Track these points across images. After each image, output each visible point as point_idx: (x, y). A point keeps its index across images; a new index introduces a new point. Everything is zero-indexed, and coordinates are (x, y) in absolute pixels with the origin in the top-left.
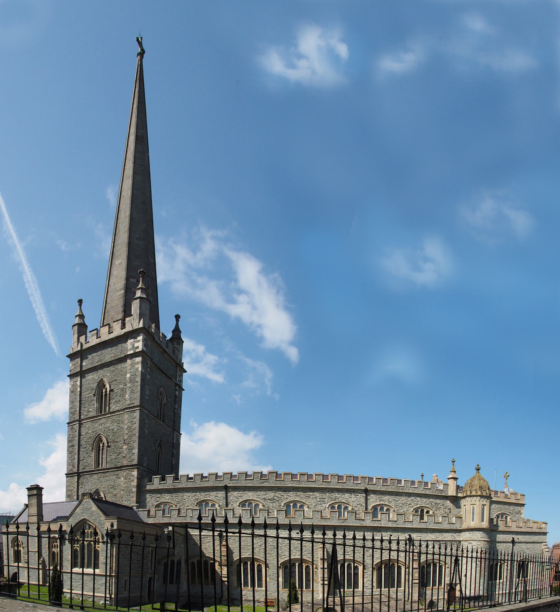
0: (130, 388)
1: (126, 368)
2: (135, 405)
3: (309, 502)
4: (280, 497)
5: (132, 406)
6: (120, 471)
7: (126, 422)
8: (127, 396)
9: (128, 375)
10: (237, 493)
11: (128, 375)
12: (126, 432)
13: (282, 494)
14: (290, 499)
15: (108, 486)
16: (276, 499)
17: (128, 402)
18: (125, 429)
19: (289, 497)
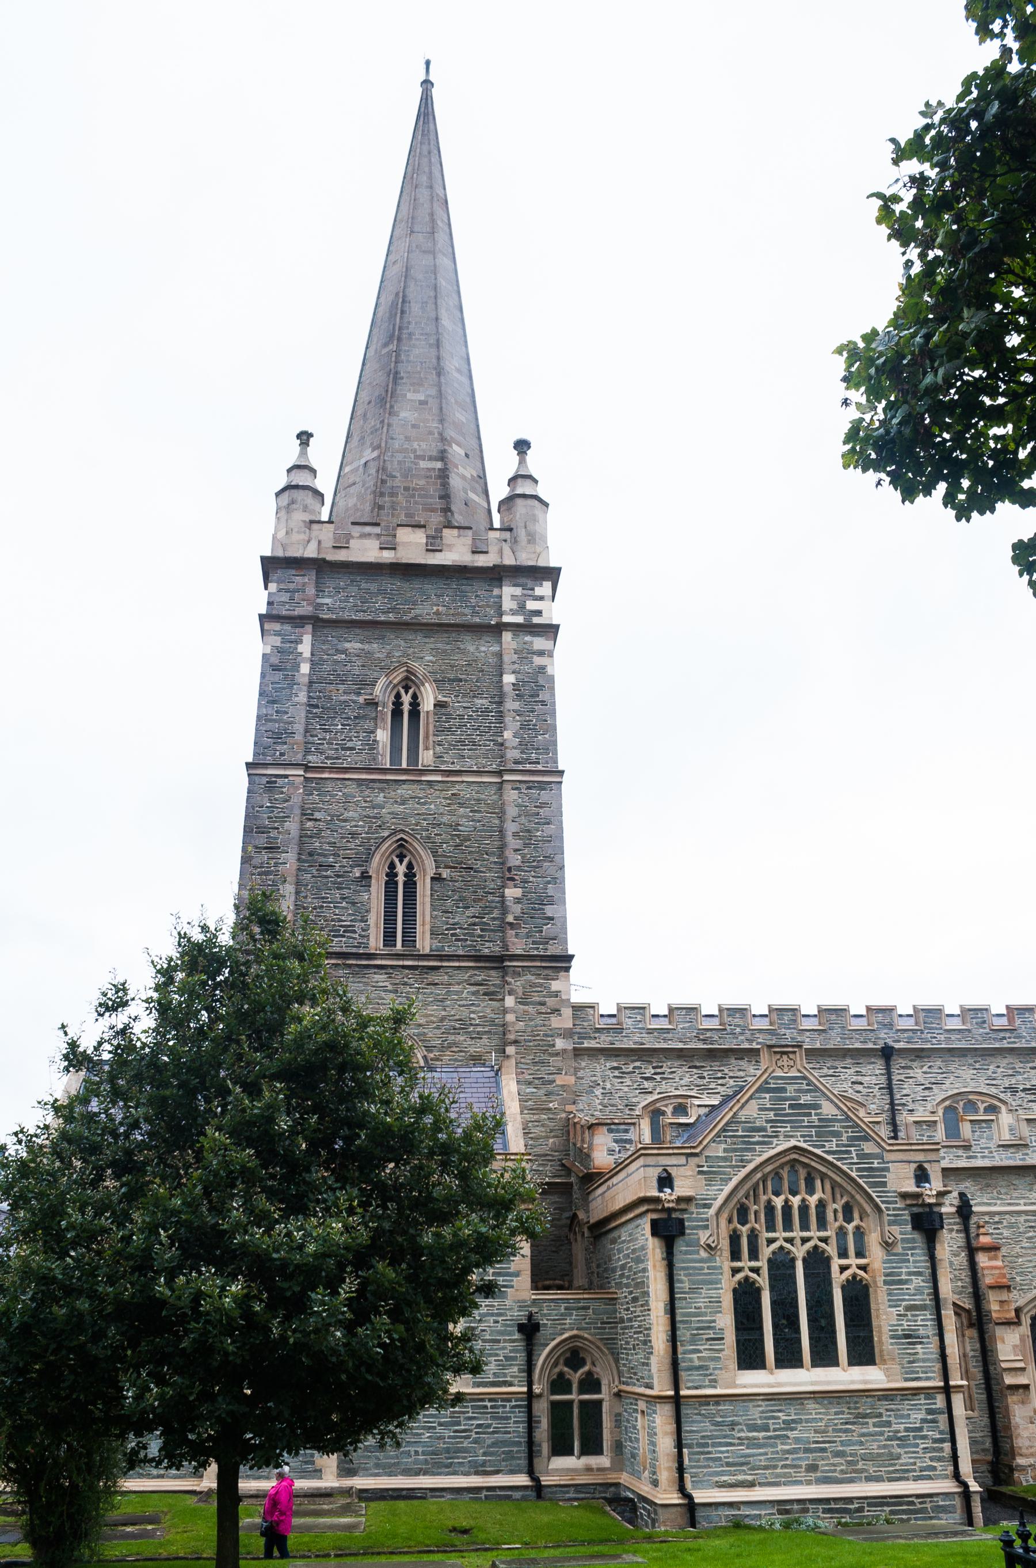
5: (528, 767)
8: (507, 735)
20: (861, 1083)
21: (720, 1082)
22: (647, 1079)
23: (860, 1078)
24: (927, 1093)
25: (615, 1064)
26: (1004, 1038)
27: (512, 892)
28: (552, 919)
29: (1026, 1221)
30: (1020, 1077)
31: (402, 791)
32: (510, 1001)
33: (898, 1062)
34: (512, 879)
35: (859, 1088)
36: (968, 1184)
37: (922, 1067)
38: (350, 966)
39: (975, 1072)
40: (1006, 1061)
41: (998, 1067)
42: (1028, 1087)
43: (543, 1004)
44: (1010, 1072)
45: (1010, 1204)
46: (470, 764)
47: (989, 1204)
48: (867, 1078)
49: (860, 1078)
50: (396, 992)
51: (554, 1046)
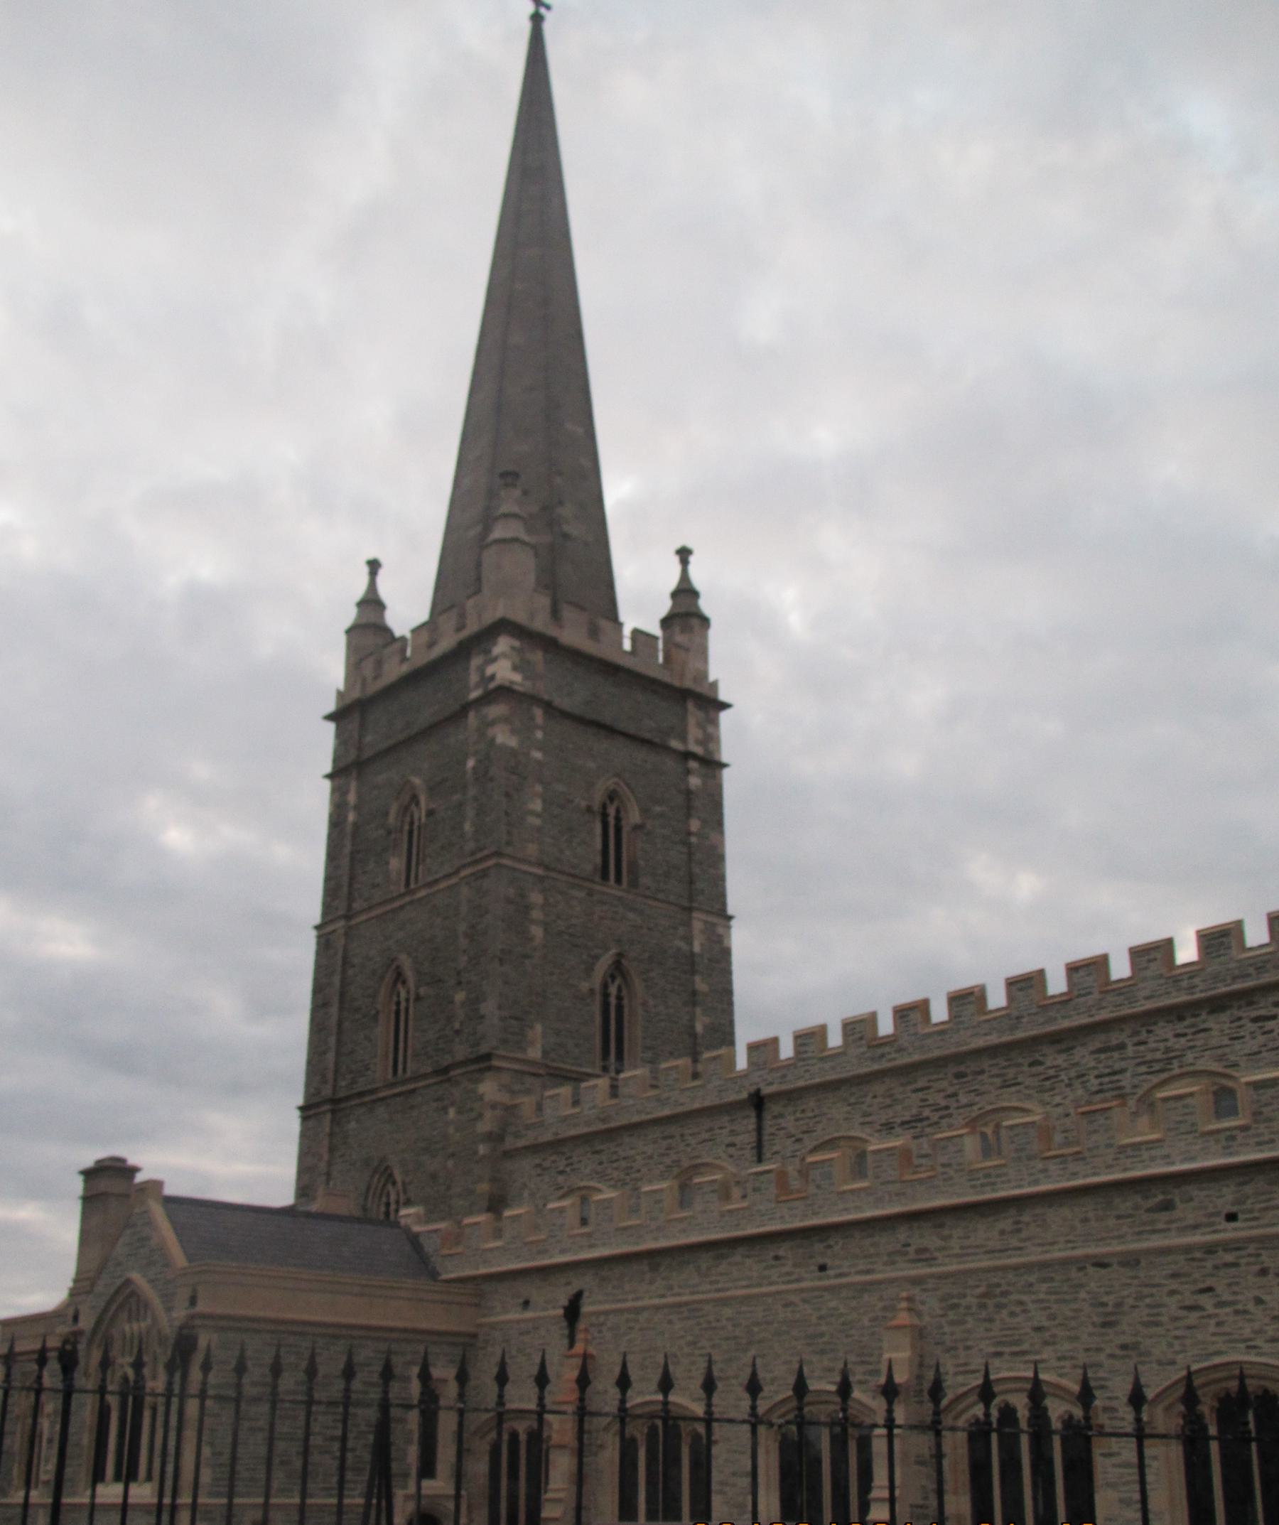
0: (476, 799)
2: (486, 852)
4: (943, 1103)
5: (479, 855)
9: (471, 763)
10: (797, 1120)
11: (471, 763)
12: (463, 943)
13: (951, 1090)
14: (978, 1106)
16: (928, 1118)
17: (470, 846)
19: (977, 1099)
21: (615, 1165)
22: (561, 1173)
24: (797, 1146)
25: (537, 1161)
26: (883, 1056)
27: (460, 996)
28: (483, 1017)
29: (627, 1321)
30: (899, 1108)
32: (452, 1113)
33: (772, 1109)
34: (459, 983)
35: (731, 1150)
37: (795, 1112)
39: (849, 1108)
41: (875, 1097)
42: (907, 1118)
43: (472, 1110)
44: (888, 1101)
45: (619, 1301)
46: (447, 869)
47: (600, 1302)
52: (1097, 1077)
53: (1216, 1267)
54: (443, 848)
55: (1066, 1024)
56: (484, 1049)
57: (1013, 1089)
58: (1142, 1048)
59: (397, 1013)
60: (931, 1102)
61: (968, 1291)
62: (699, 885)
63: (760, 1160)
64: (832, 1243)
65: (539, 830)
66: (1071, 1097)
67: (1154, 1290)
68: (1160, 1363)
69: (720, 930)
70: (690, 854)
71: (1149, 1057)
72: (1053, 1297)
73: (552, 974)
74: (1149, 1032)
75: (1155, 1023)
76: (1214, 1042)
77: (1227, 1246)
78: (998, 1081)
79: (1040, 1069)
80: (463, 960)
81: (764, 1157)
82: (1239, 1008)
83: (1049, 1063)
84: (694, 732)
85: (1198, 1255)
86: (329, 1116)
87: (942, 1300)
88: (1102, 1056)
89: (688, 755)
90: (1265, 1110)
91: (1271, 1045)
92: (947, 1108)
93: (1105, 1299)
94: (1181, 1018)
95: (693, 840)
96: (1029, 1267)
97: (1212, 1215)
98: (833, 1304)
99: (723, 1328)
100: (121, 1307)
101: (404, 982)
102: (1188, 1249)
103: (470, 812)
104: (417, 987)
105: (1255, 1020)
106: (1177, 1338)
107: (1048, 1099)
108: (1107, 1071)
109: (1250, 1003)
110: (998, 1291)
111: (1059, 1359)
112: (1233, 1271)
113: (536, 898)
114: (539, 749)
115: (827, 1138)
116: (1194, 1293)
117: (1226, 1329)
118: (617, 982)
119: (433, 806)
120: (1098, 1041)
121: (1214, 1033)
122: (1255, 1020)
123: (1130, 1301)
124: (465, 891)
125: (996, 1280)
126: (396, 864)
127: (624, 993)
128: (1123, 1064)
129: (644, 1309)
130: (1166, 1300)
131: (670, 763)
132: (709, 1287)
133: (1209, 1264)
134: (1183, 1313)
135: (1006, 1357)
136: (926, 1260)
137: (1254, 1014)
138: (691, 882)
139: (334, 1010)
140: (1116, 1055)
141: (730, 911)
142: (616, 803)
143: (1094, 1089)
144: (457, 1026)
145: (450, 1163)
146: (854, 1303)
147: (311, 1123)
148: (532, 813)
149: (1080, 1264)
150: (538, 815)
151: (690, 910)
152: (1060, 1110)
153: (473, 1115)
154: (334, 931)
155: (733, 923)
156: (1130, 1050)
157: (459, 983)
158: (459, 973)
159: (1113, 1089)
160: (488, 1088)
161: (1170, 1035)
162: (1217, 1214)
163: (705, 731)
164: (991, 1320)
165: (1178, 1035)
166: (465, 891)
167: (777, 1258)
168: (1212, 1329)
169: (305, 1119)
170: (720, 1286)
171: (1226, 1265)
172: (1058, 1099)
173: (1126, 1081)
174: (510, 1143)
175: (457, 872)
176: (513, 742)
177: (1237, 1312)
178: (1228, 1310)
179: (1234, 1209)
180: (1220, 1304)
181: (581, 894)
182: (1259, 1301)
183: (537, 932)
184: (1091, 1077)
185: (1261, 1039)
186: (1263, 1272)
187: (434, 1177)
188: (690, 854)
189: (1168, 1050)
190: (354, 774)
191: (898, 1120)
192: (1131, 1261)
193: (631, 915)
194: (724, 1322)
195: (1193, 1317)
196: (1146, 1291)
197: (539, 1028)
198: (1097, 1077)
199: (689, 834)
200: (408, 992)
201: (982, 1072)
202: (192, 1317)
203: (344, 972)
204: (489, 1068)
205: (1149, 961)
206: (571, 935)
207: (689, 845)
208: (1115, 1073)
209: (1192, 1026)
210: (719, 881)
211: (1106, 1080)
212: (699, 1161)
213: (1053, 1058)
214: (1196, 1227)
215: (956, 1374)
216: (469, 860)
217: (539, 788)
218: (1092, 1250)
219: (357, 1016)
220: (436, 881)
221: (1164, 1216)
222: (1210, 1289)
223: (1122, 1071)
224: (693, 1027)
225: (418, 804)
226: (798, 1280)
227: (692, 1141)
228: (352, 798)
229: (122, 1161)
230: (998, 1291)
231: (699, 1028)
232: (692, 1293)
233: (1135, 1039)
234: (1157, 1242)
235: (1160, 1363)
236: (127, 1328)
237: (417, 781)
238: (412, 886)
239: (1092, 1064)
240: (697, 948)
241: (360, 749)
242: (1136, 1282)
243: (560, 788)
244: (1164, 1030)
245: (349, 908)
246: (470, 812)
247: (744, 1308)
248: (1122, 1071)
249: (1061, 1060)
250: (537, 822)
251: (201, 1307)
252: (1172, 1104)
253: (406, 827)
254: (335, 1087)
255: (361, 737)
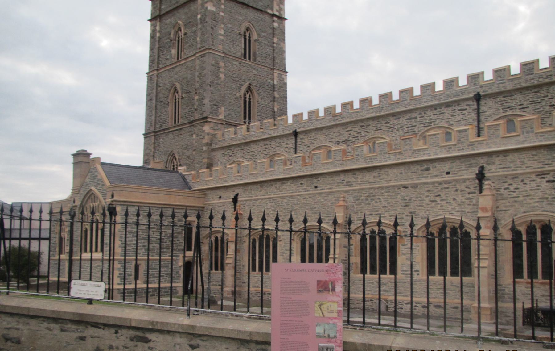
0: (201, 29)
1: (197, 8)
2: (205, 48)
3: (392, 136)
4: (356, 135)
5: (202, 49)
6: (192, 127)
7: (197, 68)
9: (199, 16)
10: (308, 140)
11: (199, 16)
12: (197, 79)
13: (359, 131)
15: (182, 146)
16: (351, 140)
17: (199, 46)
18: (196, 76)
19: (367, 134)
20: (287, 148)
21: (248, 154)
22: (230, 156)
23: (287, 146)
24: (308, 148)
25: (223, 152)
26: (337, 119)
28: (204, 104)
29: (253, 203)
30: (342, 136)
31: (177, 70)
32: (194, 136)
33: (300, 136)
35: (287, 150)
36: (240, 190)
38: (165, 133)
39: (325, 137)
40: (337, 130)
41: (334, 133)
42: (344, 140)
43: (201, 135)
44: (338, 134)
46: (192, 54)
47: (244, 197)
48: (289, 145)
49: (287, 146)
50: (174, 139)
51: (202, 149)
52: (407, 128)
53: (442, 189)
54: (190, 46)
55: (398, 110)
56: (205, 115)
57: (379, 131)
58: (422, 118)
59: (175, 103)
60: (352, 135)
61: (363, 195)
62: (277, 61)
63: (296, 153)
64: (319, 179)
65: (223, 40)
66: (398, 134)
67: (421, 196)
68: (422, 218)
69: (283, 77)
70: (274, 50)
71: (424, 121)
72: (389, 197)
73: (227, 90)
74: (425, 113)
75: (427, 111)
76: (446, 117)
77: (446, 182)
78: (375, 128)
79: (389, 125)
80: (197, 85)
81: (297, 152)
82: (455, 106)
83: (391, 123)
84: (276, 7)
85: (436, 185)
86: (153, 137)
87: (354, 197)
88: (409, 121)
89: (273, 15)
90: (461, 139)
91: (464, 118)
92: (357, 137)
93: (406, 198)
94: (436, 109)
95: (275, 45)
96: (382, 188)
97: (442, 172)
98: (319, 198)
99: (283, 206)
100: (89, 198)
101: (177, 93)
102: (433, 183)
103: (199, 34)
104: (182, 94)
105: (459, 110)
106: (428, 210)
107: (391, 135)
108: (410, 126)
109: (459, 105)
110: (372, 195)
111: (390, 216)
112: (447, 190)
113: (222, 64)
114: (223, 12)
115: (318, 146)
116: (434, 197)
117: (443, 208)
118: (249, 93)
119: (186, 31)
120: (408, 116)
121: (446, 114)
122: (459, 110)
123: (414, 199)
124: (198, 62)
125: (371, 192)
126: (174, 52)
127: (251, 97)
128: (416, 124)
129: (258, 199)
130: (425, 199)
131: (268, 18)
132: (279, 193)
133: (440, 188)
134: (431, 203)
135: (374, 215)
136: (350, 185)
137: (459, 108)
138: (274, 60)
139: (154, 102)
140: (413, 120)
141: (287, 70)
142: (249, 32)
143: (406, 131)
144: (196, 108)
145: (194, 153)
146: (326, 198)
147: (147, 139)
148: (220, 34)
149: (398, 187)
150: (222, 35)
151: (273, 69)
152: (394, 138)
153: (201, 137)
154: (153, 75)
155: (287, 74)
156: (418, 119)
157: (196, 93)
158: (196, 90)
159: (412, 132)
160: (207, 128)
161: (432, 114)
162: (444, 172)
163: (280, 7)
164: (369, 204)
165: (434, 115)
166: (198, 62)
167: (301, 184)
168: (439, 208)
169: (145, 138)
170: (283, 192)
171: (445, 188)
172: (394, 135)
173: (416, 129)
174: (214, 146)
175: (195, 55)
176: (213, 9)
177: (447, 203)
178: (445, 202)
179: (448, 171)
180: (442, 200)
181: (237, 63)
182: (454, 199)
183: (222, 76)
184: (405, 128)
185: (461, 116)
186: (457, 190)
187: (189, 157)
188: (274, 50)
189: (430, 120)
190: (158, 19)
191: (341, 141)
192: (415, 186)
193: (254, 71)
194: (284, 204)
195: (433, 204)
196: (419, 196)
197: (223, 108)
198: (407, 128)
199: (274, 43)
200: (179, 96)
201: (369, 125)
202: (112, 201)
203: (157, 89)
204: (207, 122)
205: (427, 90)
206: (234, 77)
207: (273, 47)
208: (413, 126)
209: (439, 112)
210: (283, 60)
211: (410, 128)
212: (276, 153)
213: (393, 121)
214: (436, 176)
215: (357, 220)
216: (199, 50)
217: (223, 26)
218: (403, 183)
219: (162, 104)
220: (187, 58)
221: (427, 172)
222: (439, 195)
223: (415, 126)
224: (274, 109)
225: (181, 30)
226: (307, 191)
227: (274, 146)
228: (158, 28)
229: (86, 151)
230: (372, 195)
231: (276, 109)
232: (274, 195)
233: (420, 116)
234: (423, 180)
235: (422, 218)
236: (91, 205)
237: (180, 22)
238: (180, 59)
239: (406, 123)
240: (275, 83)
241: (160, 11)
242: (416, 193)
243: (230, 26)
244: (430, 113)
245: (158, 67)
246: (199, 34)
247: (291, 200)
248: (415, 126)
249: (395, 122)
250: (222, 38)
251: (115, 198)
252: (432, 137)
253: (177, 39)
254: (155, 128)
255: (161, 6)
